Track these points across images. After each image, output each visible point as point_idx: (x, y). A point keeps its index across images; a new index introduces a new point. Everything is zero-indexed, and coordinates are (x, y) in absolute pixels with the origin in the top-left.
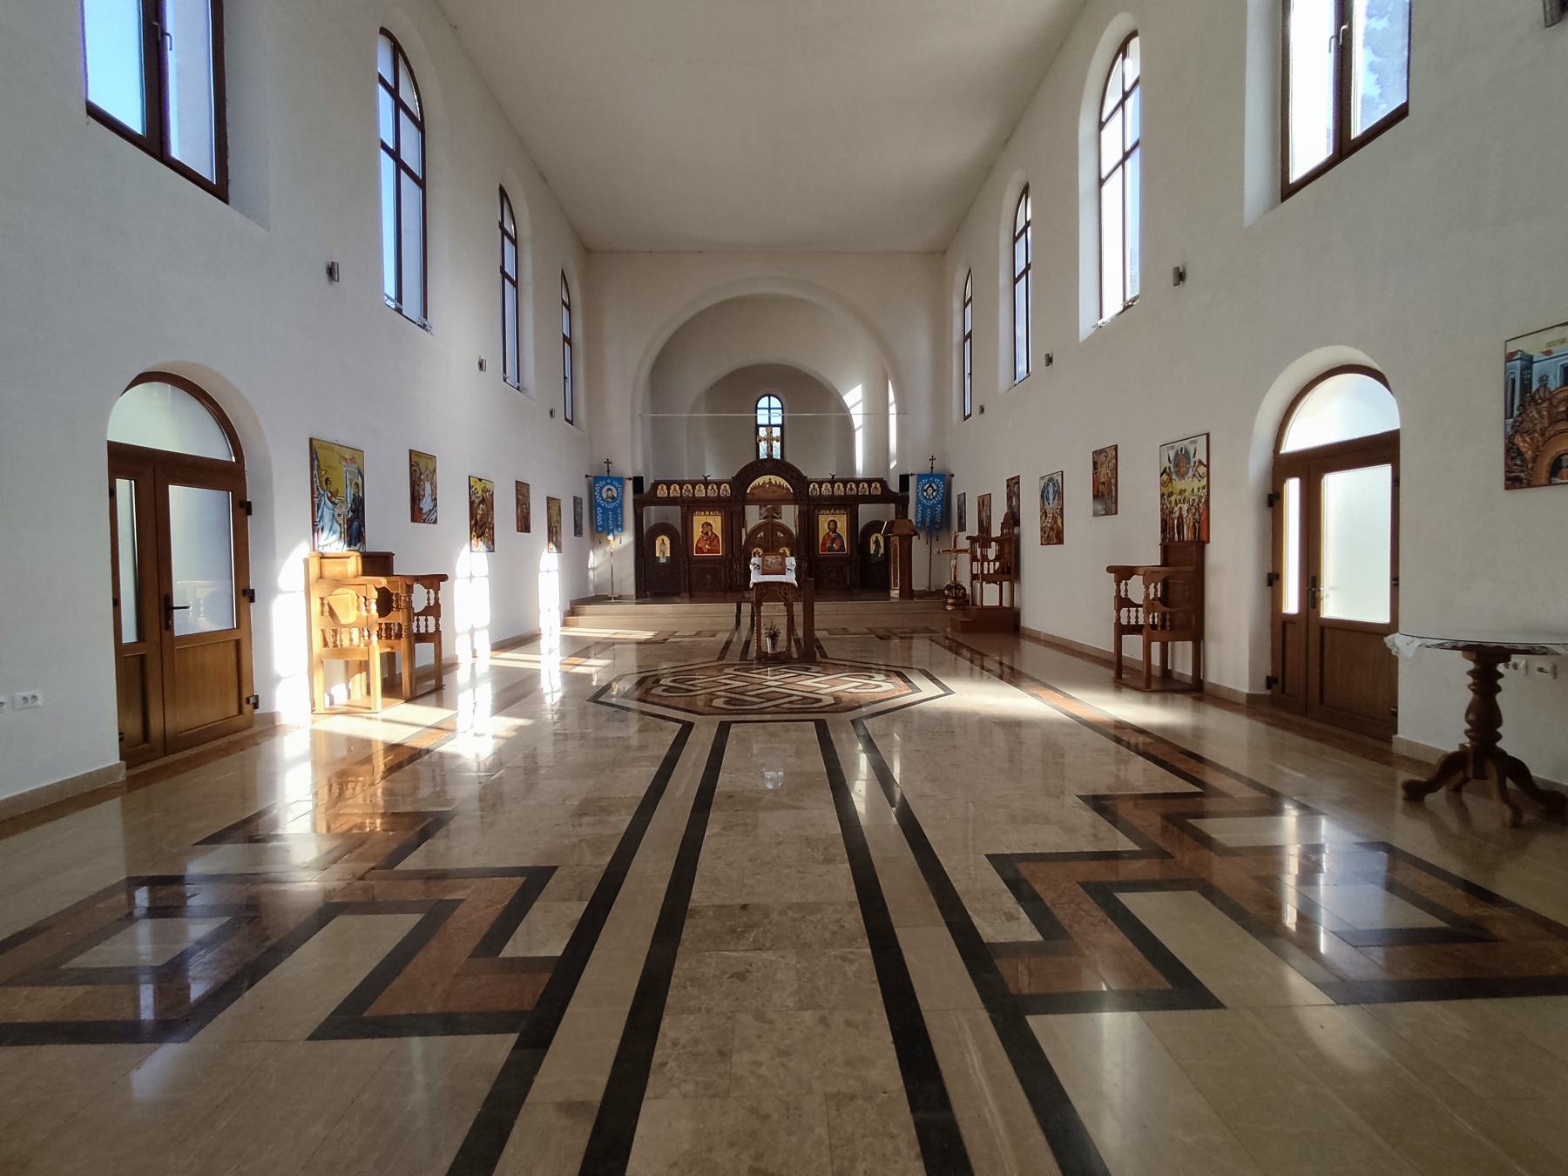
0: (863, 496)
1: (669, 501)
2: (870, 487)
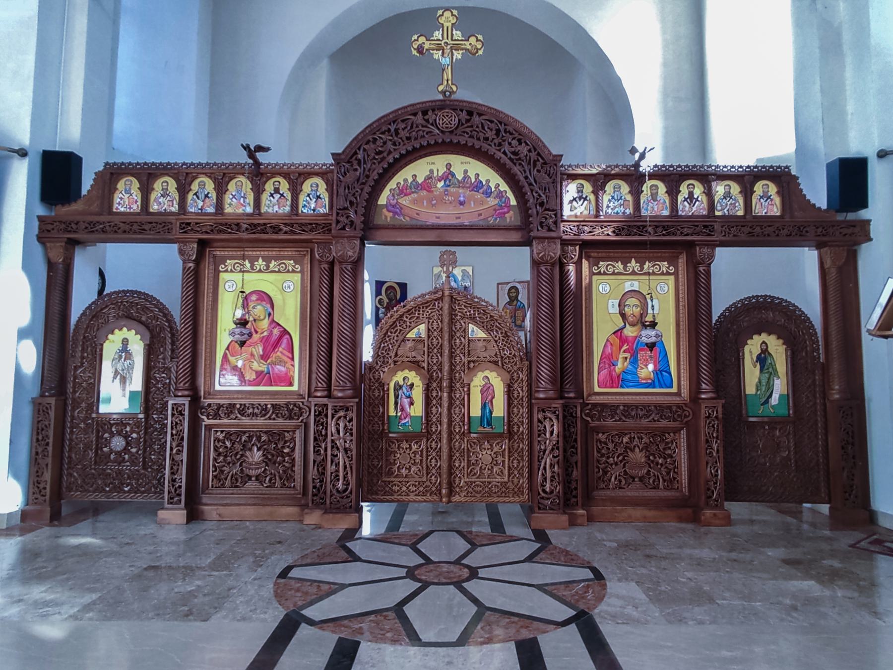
0: (729, 221)
2: (748, 193)
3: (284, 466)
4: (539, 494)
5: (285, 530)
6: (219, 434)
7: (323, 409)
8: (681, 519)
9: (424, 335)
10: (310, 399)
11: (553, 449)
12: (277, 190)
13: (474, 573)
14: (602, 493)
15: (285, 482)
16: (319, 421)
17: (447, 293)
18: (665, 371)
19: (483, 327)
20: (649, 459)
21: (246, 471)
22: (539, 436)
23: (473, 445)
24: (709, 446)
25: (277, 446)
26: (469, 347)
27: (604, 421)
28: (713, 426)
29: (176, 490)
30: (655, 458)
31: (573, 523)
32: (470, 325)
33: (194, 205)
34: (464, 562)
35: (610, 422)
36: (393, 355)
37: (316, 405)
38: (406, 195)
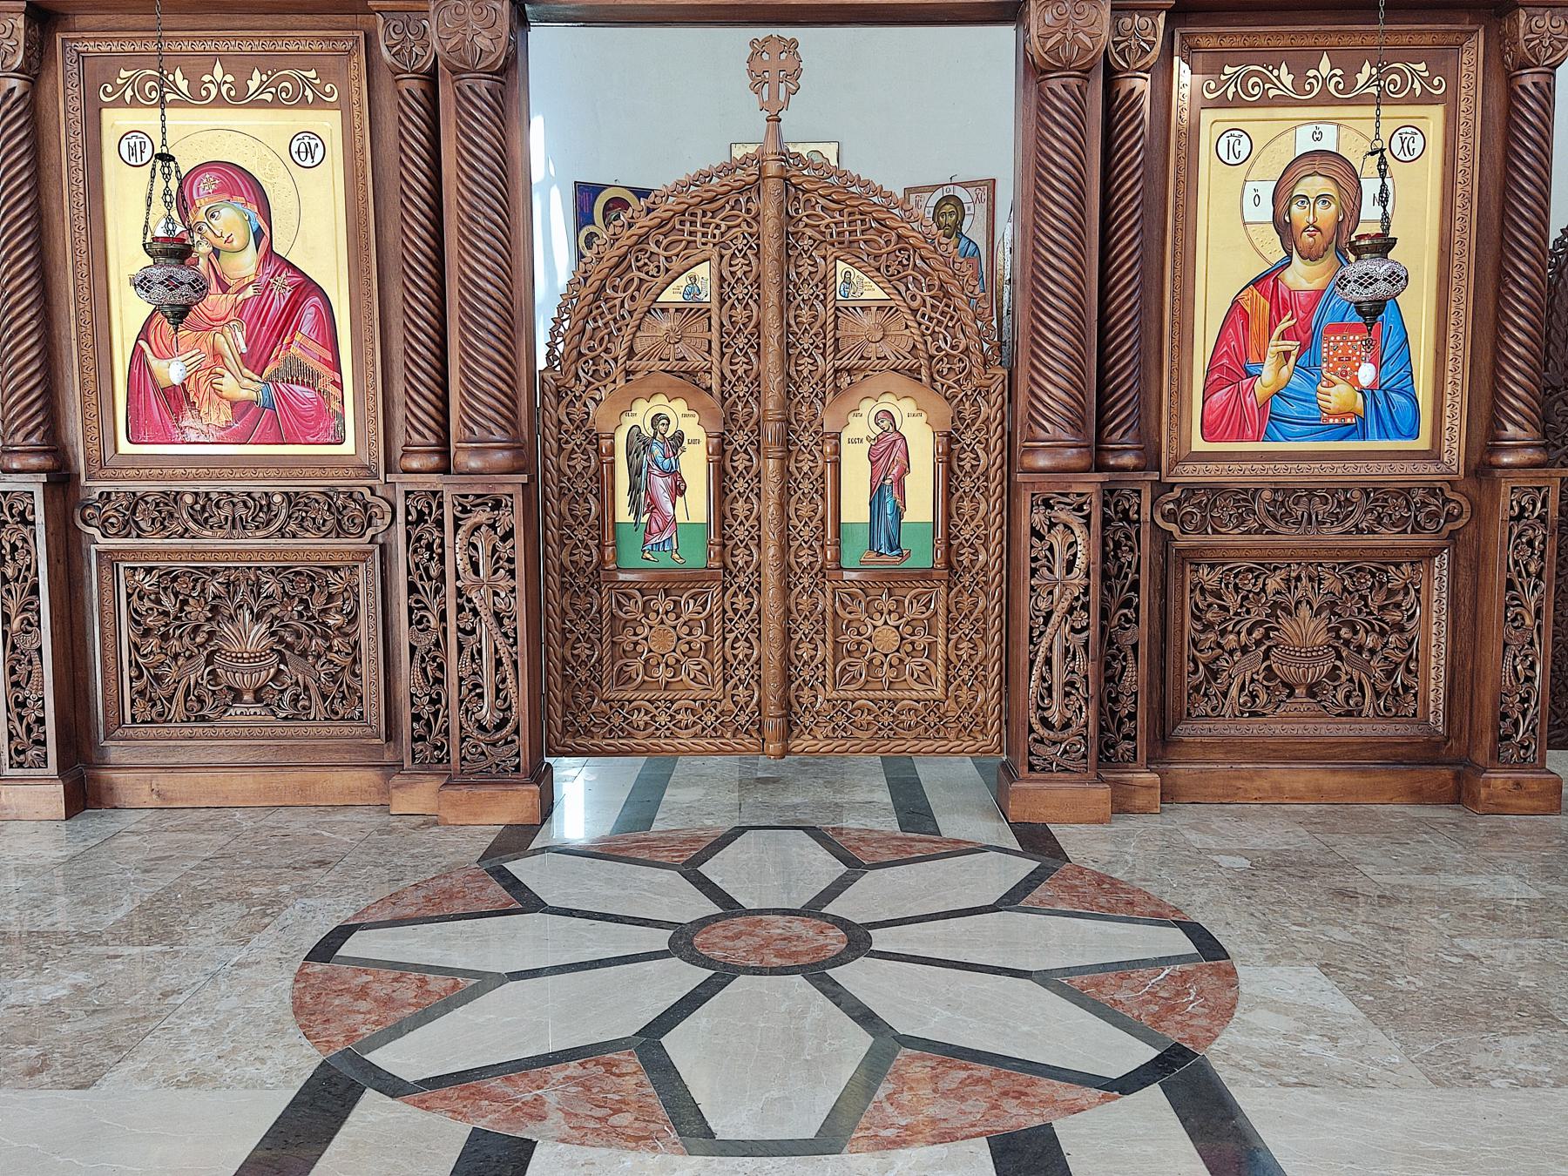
3: (331, 662)
4: (1031, 730)
5: (346, 830)
6: (140, 576)
7: (430, 507)
8: (1419, 796)
9: (707, 292)
10: (391, 478)
11: (1071, 610)
13: (858, 941)
14: (1202, 727)
15: (337, 705)
16: (419, 539)
17: (772, 168)
18: (1400, 392)
19: (878, 270)
20: (1338, 637)
21: (226, 677)
22: (1034, 572)
23: (847, 599)
24: (1513, 598)
25: (307, 608)
26: (836, 328)
27: (1215, 531)
28: (1530, 543)
29: (29, 730)
30: (1356, 632)
31: (1121, 808)
32: (841, 266)
35: (1233, 537)
36: (622, 353)
37: (407, 493)
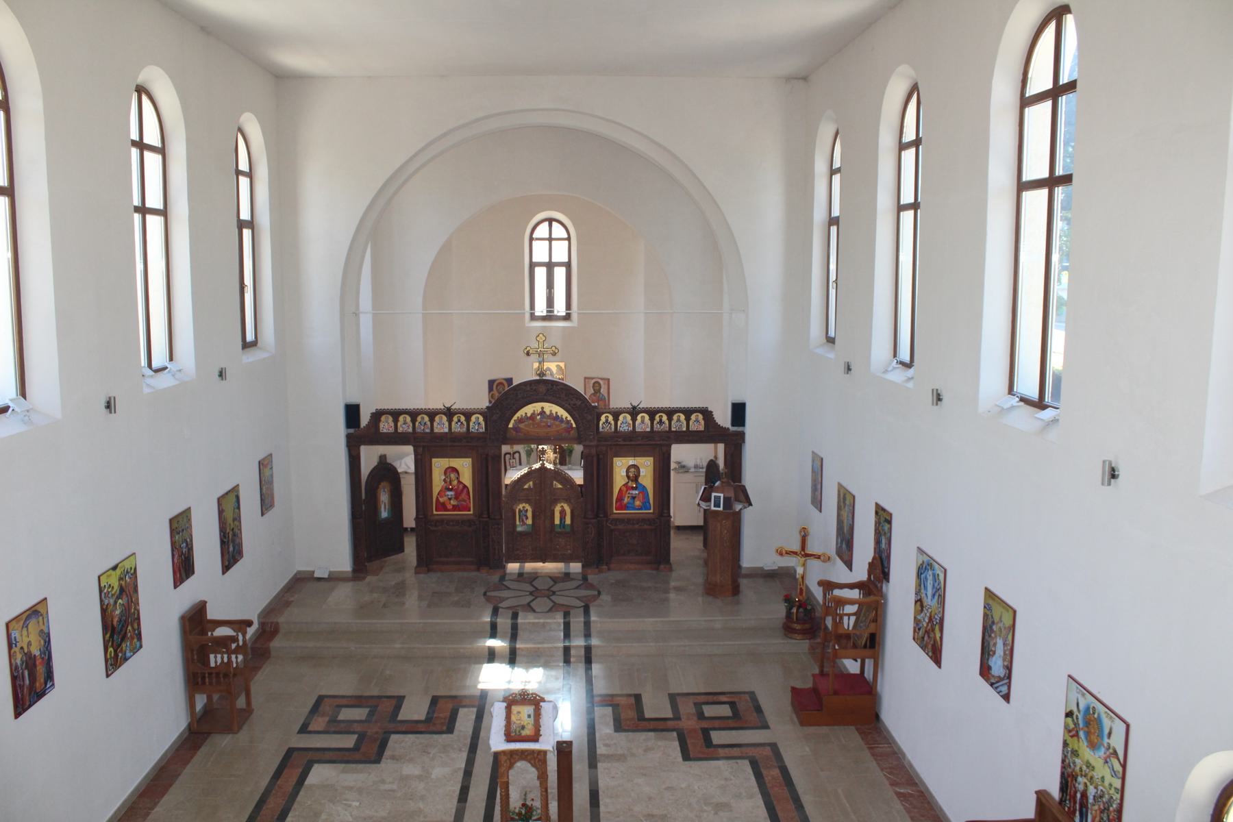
1: (397, 439)
2: (688, 419)
12: (459, 421)
13: (554, 593)
33: (419, 428)
34: (552, 589)
35: (620, 527)
38: (523, 422)
